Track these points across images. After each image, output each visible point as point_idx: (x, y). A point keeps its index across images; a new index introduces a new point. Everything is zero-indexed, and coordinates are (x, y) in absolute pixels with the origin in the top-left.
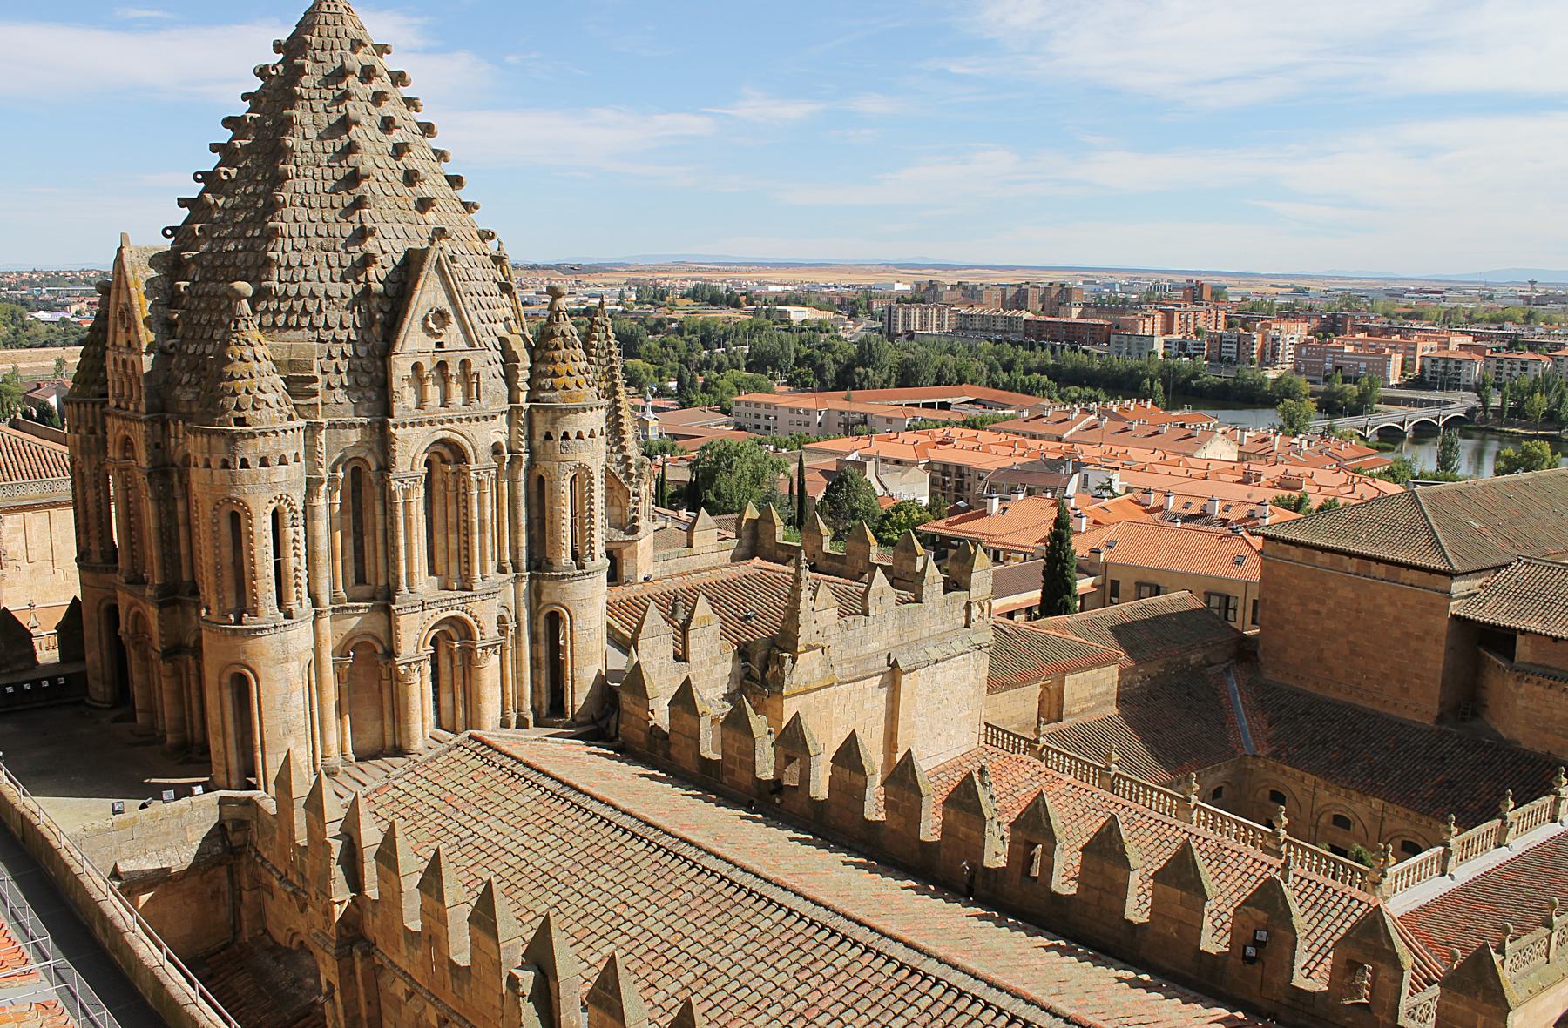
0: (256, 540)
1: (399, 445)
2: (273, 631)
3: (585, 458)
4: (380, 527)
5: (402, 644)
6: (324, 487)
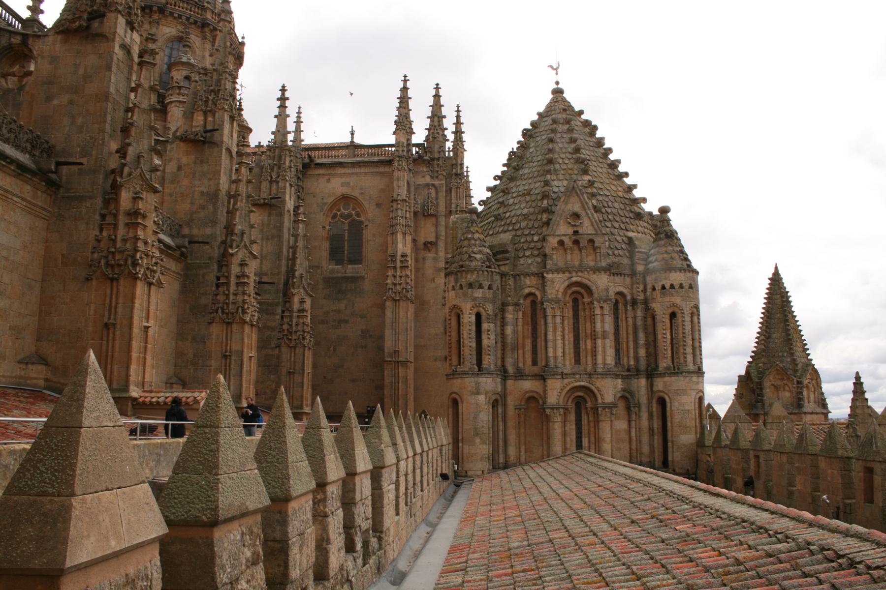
1: (548, 284)
3: (677, 300)
4: (543, 332)
5: (549, 397)
6: (511, 308)
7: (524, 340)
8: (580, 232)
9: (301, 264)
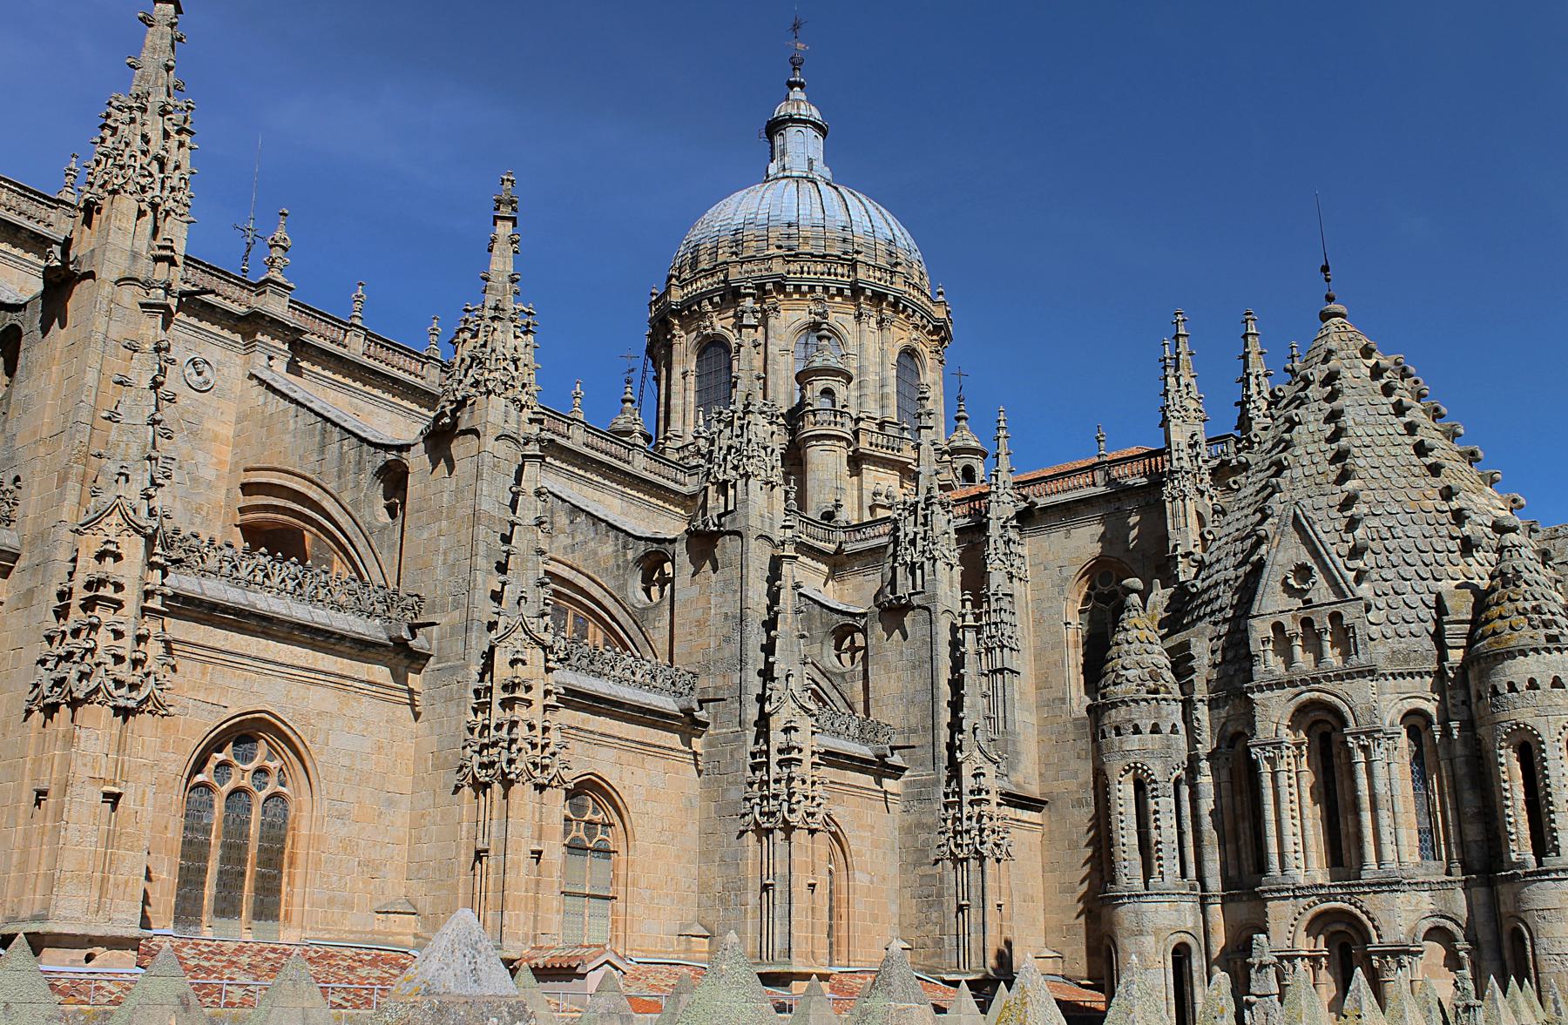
0: (1112, 808)
1: (1258, 710)
2: (1126, 900)
3: (1525, 716)
7: (1236, 823)
8: (1316, 601)
9: (973, 706)
